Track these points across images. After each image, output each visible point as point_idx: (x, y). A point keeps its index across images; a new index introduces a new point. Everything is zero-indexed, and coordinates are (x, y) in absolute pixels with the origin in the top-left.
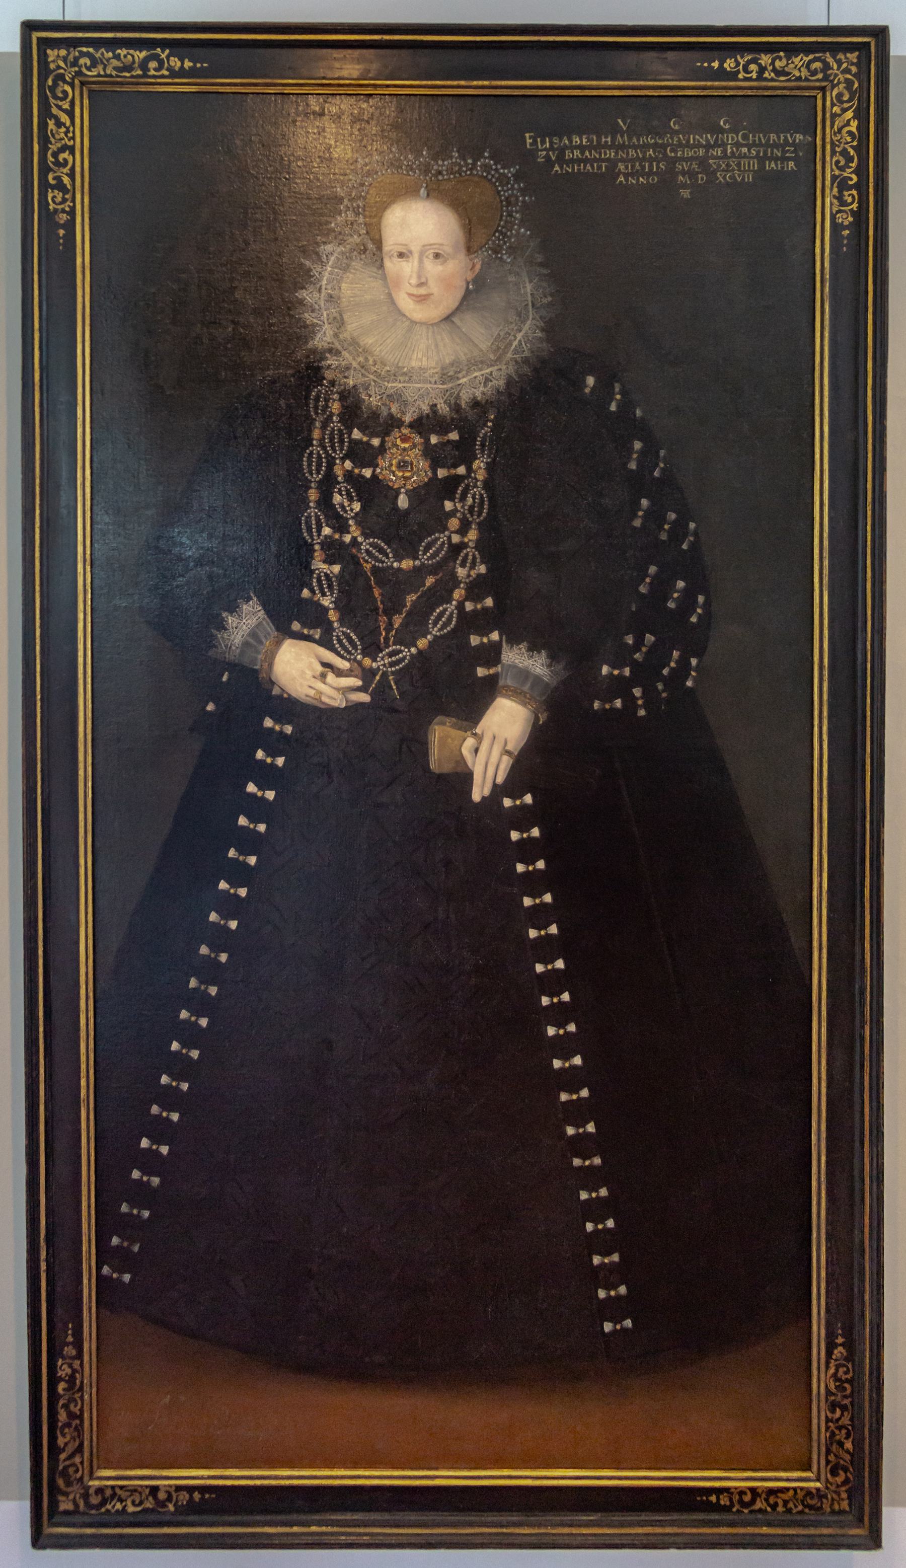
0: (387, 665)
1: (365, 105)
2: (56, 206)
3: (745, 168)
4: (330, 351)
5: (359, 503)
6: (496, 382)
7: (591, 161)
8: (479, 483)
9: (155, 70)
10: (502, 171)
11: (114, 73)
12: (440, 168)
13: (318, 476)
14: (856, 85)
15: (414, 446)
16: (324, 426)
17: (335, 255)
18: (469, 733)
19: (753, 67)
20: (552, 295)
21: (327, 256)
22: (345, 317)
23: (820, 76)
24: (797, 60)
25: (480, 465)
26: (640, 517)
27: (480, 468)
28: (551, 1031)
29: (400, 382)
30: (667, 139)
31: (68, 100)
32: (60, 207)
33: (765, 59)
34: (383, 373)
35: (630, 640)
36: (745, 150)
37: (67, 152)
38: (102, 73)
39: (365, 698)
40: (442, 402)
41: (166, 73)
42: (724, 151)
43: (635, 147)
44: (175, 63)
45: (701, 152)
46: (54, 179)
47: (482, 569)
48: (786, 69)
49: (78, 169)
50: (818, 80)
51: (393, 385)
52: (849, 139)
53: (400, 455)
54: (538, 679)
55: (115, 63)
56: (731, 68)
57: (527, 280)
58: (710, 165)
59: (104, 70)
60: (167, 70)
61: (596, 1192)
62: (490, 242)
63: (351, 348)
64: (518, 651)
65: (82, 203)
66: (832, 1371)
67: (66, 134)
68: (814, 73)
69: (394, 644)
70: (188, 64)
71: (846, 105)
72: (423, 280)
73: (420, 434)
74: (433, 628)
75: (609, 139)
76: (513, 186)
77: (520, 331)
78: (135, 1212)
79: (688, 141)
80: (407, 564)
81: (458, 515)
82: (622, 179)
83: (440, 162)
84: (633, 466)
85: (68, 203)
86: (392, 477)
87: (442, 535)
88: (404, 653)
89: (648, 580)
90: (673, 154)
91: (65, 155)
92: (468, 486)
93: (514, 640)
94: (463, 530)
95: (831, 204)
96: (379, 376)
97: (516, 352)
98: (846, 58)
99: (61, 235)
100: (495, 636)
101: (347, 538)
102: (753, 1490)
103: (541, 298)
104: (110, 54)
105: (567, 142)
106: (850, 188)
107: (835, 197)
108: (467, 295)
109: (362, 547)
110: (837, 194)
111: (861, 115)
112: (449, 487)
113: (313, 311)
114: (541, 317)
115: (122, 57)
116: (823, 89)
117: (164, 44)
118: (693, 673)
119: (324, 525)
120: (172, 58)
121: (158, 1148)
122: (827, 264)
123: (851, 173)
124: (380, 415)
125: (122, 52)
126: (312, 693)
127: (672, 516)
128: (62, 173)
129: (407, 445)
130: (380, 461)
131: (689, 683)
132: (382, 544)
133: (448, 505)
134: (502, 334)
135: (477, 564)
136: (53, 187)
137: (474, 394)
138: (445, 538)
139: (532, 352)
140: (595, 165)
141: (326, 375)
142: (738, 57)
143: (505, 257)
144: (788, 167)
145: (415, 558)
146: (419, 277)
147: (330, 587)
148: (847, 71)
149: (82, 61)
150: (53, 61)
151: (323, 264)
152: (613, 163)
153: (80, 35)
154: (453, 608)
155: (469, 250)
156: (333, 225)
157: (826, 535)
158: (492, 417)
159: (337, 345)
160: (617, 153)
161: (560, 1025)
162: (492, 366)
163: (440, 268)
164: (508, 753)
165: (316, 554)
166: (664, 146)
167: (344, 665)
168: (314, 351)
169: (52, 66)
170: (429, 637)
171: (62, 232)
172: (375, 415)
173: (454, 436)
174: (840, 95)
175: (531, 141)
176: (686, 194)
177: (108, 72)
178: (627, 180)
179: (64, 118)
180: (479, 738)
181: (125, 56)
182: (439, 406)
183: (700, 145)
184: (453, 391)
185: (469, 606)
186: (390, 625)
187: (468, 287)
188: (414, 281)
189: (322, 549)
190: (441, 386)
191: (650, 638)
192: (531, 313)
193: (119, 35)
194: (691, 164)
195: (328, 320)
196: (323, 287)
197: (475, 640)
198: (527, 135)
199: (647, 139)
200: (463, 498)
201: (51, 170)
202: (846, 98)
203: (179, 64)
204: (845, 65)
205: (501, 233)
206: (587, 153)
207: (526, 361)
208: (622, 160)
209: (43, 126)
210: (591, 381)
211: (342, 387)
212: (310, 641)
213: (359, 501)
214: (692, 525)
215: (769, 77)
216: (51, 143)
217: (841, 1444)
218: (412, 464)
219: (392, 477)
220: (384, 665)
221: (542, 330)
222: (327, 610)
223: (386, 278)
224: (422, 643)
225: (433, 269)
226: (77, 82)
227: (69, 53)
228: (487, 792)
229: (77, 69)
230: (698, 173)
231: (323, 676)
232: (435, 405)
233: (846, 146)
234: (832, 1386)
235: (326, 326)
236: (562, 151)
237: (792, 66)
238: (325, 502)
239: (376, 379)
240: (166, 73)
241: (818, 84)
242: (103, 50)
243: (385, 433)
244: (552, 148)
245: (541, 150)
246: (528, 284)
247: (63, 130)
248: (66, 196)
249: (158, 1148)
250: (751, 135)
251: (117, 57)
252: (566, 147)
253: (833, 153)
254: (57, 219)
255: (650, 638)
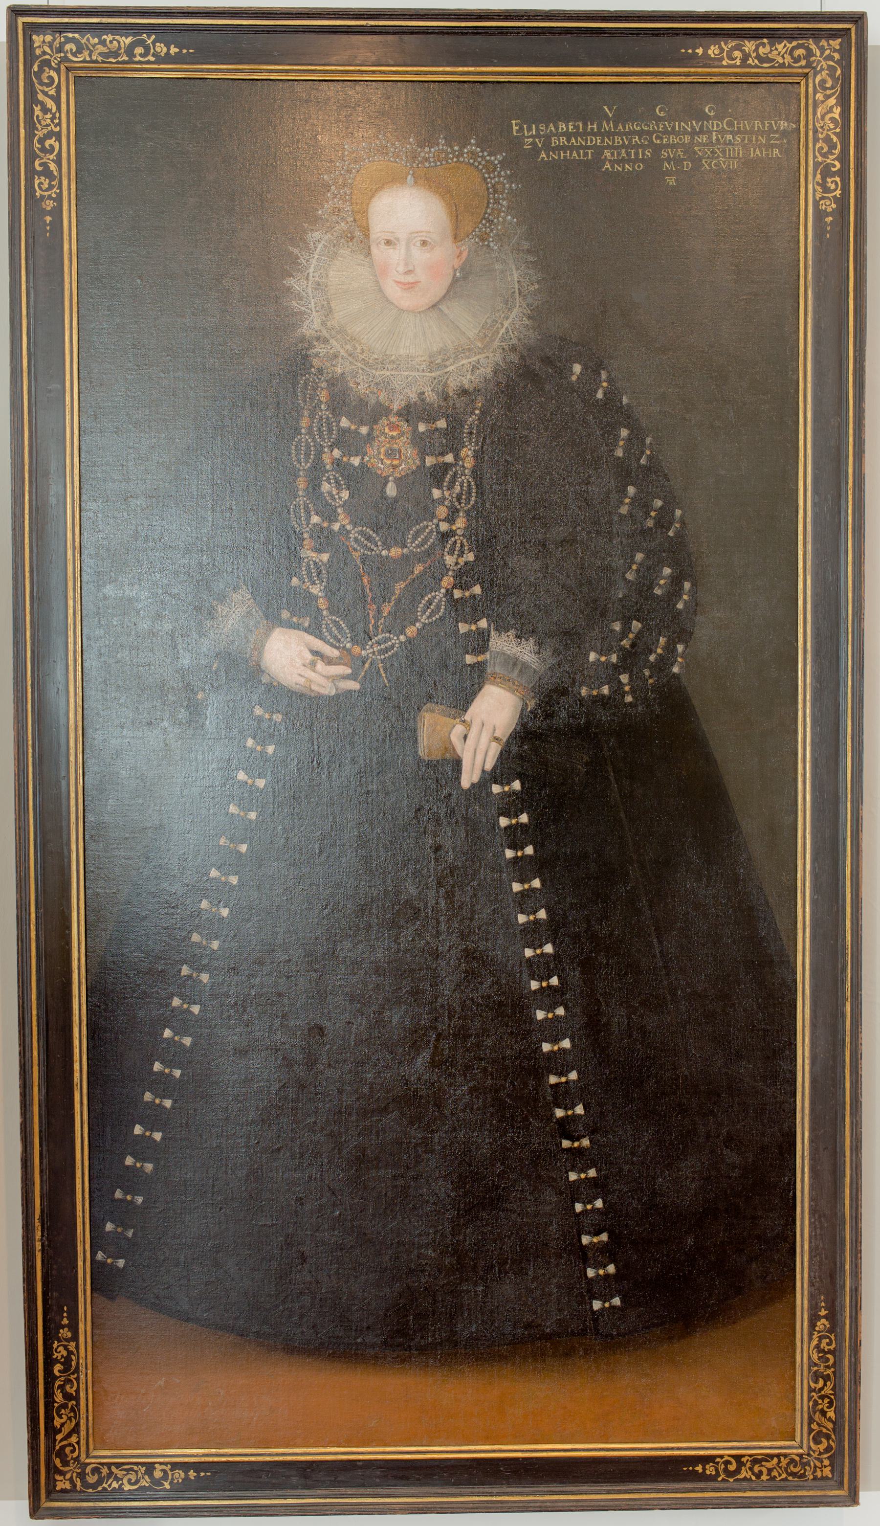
0: (376, 653)
1: (351, 92)
2: (43, 193)
3: (729, 155)
4: (318, 339)
5: (348, 492)
6: (484, 370)
7: (578, 148)
8: (466, 471)
9: (141, 55)
10: (488, 158)
11: (100, 59)
12: (427, 155)
13: (306, 464)
14: (839, 72)
15: (402, 434)
16: (311, 416)
17: (323, 242)
18: (458, 720)
19: (737, 54)
20: (538, 282)
21: (314, 244)
22: (333, 304)
23: (803, 63)
24: (780, 47)
25: (467, 453)
26: (627, 504)
27: (468, 456)
28: (540, 1015)
29: (388, 370)
30: (652, 126)
31: (54, 86)
32: (46, 194)
33: (749, 46)
34: (371, 362)
35: (617, 627)
36: (729, 137)
37: (54, 139)
38: (88, 59)
39: (354, 685)
40: (430, 390)
41: (152, 59)
42: (710, 138)
43: (619, 134)
44: (161, 49)
45: (687, 139)
46: (40, 165)
47: (471, 557)
48: (769, 55)
49: (64, 155)
50: (801, 67)
51: (382, 373)
52: (832, 126)
53: (389, 443)
54: (525, 666)
55: (101, 48)
56: (715, 54)
57: (514, 267)
58: (695, 153)
59: (90, 55)
60: (153, 55)
61: (584, 1173)
62: (477, 230)
63: (339, 337)
64: (507, 639)
65: (69, 189)
66: (815, 1342)
67: (52, 119)
68: (797, 60)
69: (383, 632)
70: (174, 50)
71: (829, 92)
72: (411, 268)
73: (408, 422)
74: (422, 615)
75: (595, 126)
76: (499, 173)
77: (507, 318)
78: (129, 1198)
79: (674, 128)
80: (395, 552)
81: (446, 503)
82: (608, 166)
83: (427, 149)
84: (619, 453)
85: (55, 189)
86: (380, 465)
87: (430, 523)
88: (393, 641)
89: (634, 567)
90: (658, 142)
91: (52, 141)
92: (455, 473)
93: (502, 628)
94: (451, 519)
95: (814, 191)
96: (367, 364)
97: (503, 339)
98: (829, 45)
99: (48, 222)
100: (483, 623)
101: (336, 527)
102: (738, 1458)
103: (528, 285)
104: (96, 40)
105: (553, 129)
106: (834, 174)
107: (818, 183)
108: (455, 281)
109: (351, 535)
110: (820, 181)
111: (844, 102)
112: (438, 475)
113: (301, 299)
114: (528, 306)
115: (108, 42)
116: (806, 75)
117: (151, 28)
118: (679, 660)
119: (312, 513)
120: (158, 44)
121: (151, 1134)
122: (810, 251)
123: (833, 160)
124: (367, 403)
125: (108, 38)
126: (302, 681)
127: (658, 503)
128: (49, 159)
129: (395, 433)
130: (369, 450)
131: (676, 670)
132: (371, 533)
133: (436, 493)
134: (489, 321)
135: (466, 552)
136: (40, 174)
137: (461, 382)
138: (434, 526)
139: (519, 340)
140: (582, 151)
141: (314, 363)
142: (722, 43)
143: (492, 244)
144: (772, 155)
145: (404, 546)
146: (406, 265)
147: (319, 573)
148: (830, 58)
149: (68, 47)
150: (39, 47)
151: (311, 252)
152: (599, 151)
153: (66, 20)
154: (441, 595)
155: (456, 237)
156: (320, 212)
157: (809, 520)
158: (480, 405)
159: (325, 333)
160: (603, 141)
161: (550, 1008)
162: (479, 353)
163: (428, 255)
164: (496, 739)
165: (306, 542)
166: (650, 133)
167: (333, 653)
168: (303, 339)
169: (38, 52)
170: (418, 624)
171: (48, 219)
172: (363, 403)
173: (442, 424)
174: (823, 81)
175: (517, 128)
176: (671, 181)
177: (94, 58)
178: (613, 167)
179: (50, 104)
180: (467, 725)
181: (111, 42)
182: (426, 394)
183: (685, 132)
184: (440, 379)
185: (457, 594)
186: (379, 611)
187: (455, 275)
188: (401, 269)
189: (311, 537)
190: (428, 374)
191: (636, 625)
192: (517, 300)
193: (105, 20)
194: (677, 151)
195: (315, 307)
196: (311, 275)
197: (463, 628)
198: (514, 122)
199: (633, 126)
200: (451, 487)
201: (38, 156)
202: (829, 84)
203: (165, 50)
204: (827, 52)
205: (489, 221)
206: (573, 140)
207: (513, 349)
208: (608, 147)
209: (29, 112)
210: (577, 368)
211: (330, 375)
212: (298, 629)
213: (348, 489)
214: (678, 513)
215: (753, 64)
216: (37, 130)
217: (823, 1413)
218: (400, 452)
219: (380, 465)
220: (374, 652)
221: (530, 317)
222: (316, 598)
223: (373, 265)
224: (411, 631)
225: (420, 256)
226: (62, 68)
227: (54, 40)
228: (476, 779)
229: (62, 55)
230: (685, 160)
231: (313, 665)
232: (423, 393)
233: (829, 133)
234: (815, 1357)
235: (314, 313)
236: (548, 137)
237: (775, 52)
238: (314, 487)
239: (363, 366)
240: (152, 59)
241: (800, 71)
242: (89, 35)
243: (374, 420)
244: (538, 136)
245: (528, 137)
246: (514, 271)
247: (49, 116)
248: (52, 183)
249: (151, 1134)
250: (736, 122)
251: (103, 43)
252: (552, 134)
253: (816, 140)
254: (44, 206)
255: (636, 625)
